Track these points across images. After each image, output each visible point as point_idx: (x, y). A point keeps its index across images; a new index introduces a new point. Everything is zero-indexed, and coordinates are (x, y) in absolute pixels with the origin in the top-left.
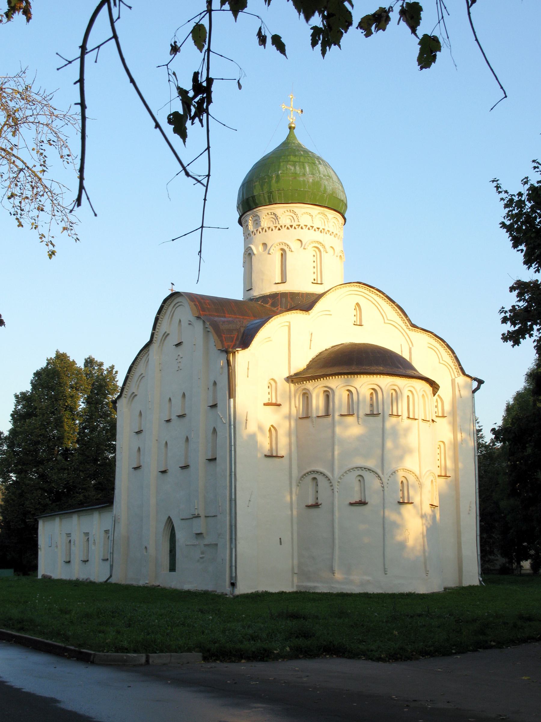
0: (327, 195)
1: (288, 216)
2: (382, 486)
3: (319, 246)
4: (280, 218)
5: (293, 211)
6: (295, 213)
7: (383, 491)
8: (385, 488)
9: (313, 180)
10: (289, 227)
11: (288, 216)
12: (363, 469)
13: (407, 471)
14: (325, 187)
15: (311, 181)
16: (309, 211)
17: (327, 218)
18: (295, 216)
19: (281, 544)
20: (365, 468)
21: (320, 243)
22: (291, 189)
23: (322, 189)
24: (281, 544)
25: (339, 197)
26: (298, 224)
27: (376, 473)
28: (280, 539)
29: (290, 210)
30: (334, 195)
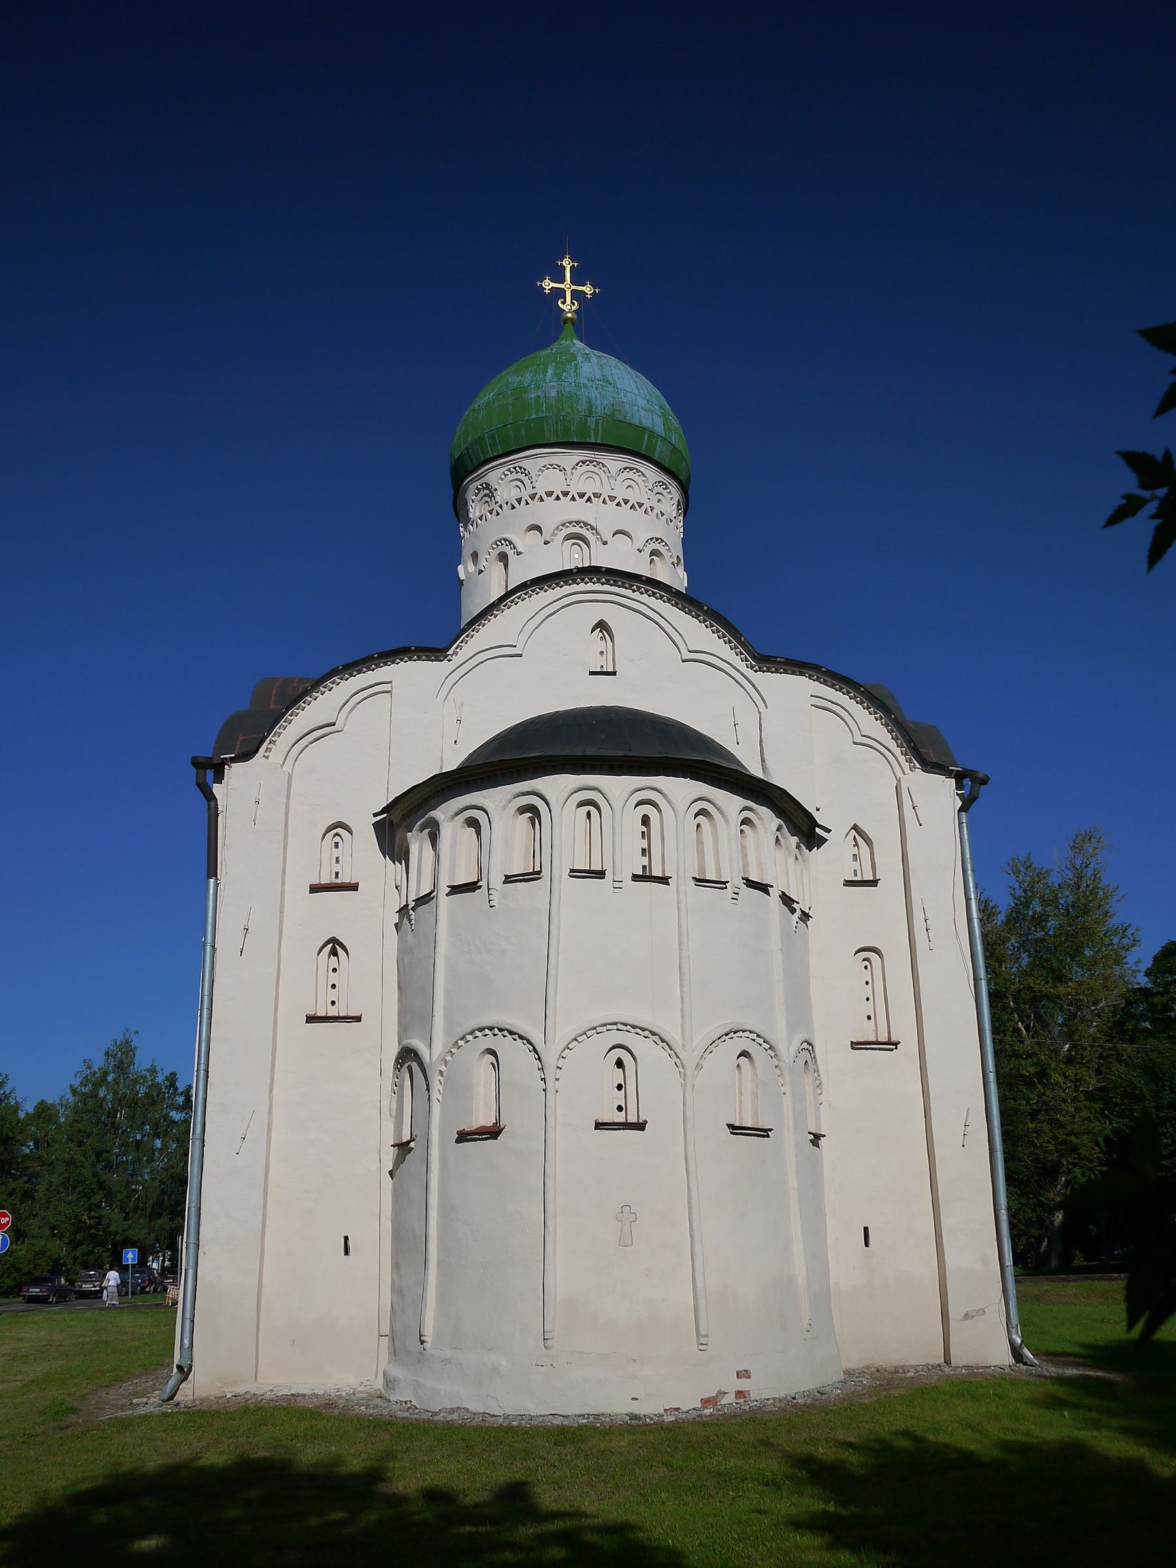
0: (597, 422)
1: (511, 481)
2: (543, 1077)
3: (577, 530)
4: (496, 490)
5: (520, 468)
6: (523, 470)
7: (545, 1090)
8: (550, 1082)
9: (558, 392)
10: (516, 504)
11: (511, 481)
12: (496, 1031)
13: (624, 1028)
14: (590, 401)
15: (553, 394)
16: (554, 460)
17: (605, 469)
18: (525, 479)
19: (347, 1253)
20: (501, 1030)
21: (586, 524)
22: (510, 421)
23: (582, 406)
24: (347, 1253)
25: (636, 422)
26: (534, 491)
27: (529, 1042)
28: (346, 1238)
29: (515, 468)
30: (619, 417)
